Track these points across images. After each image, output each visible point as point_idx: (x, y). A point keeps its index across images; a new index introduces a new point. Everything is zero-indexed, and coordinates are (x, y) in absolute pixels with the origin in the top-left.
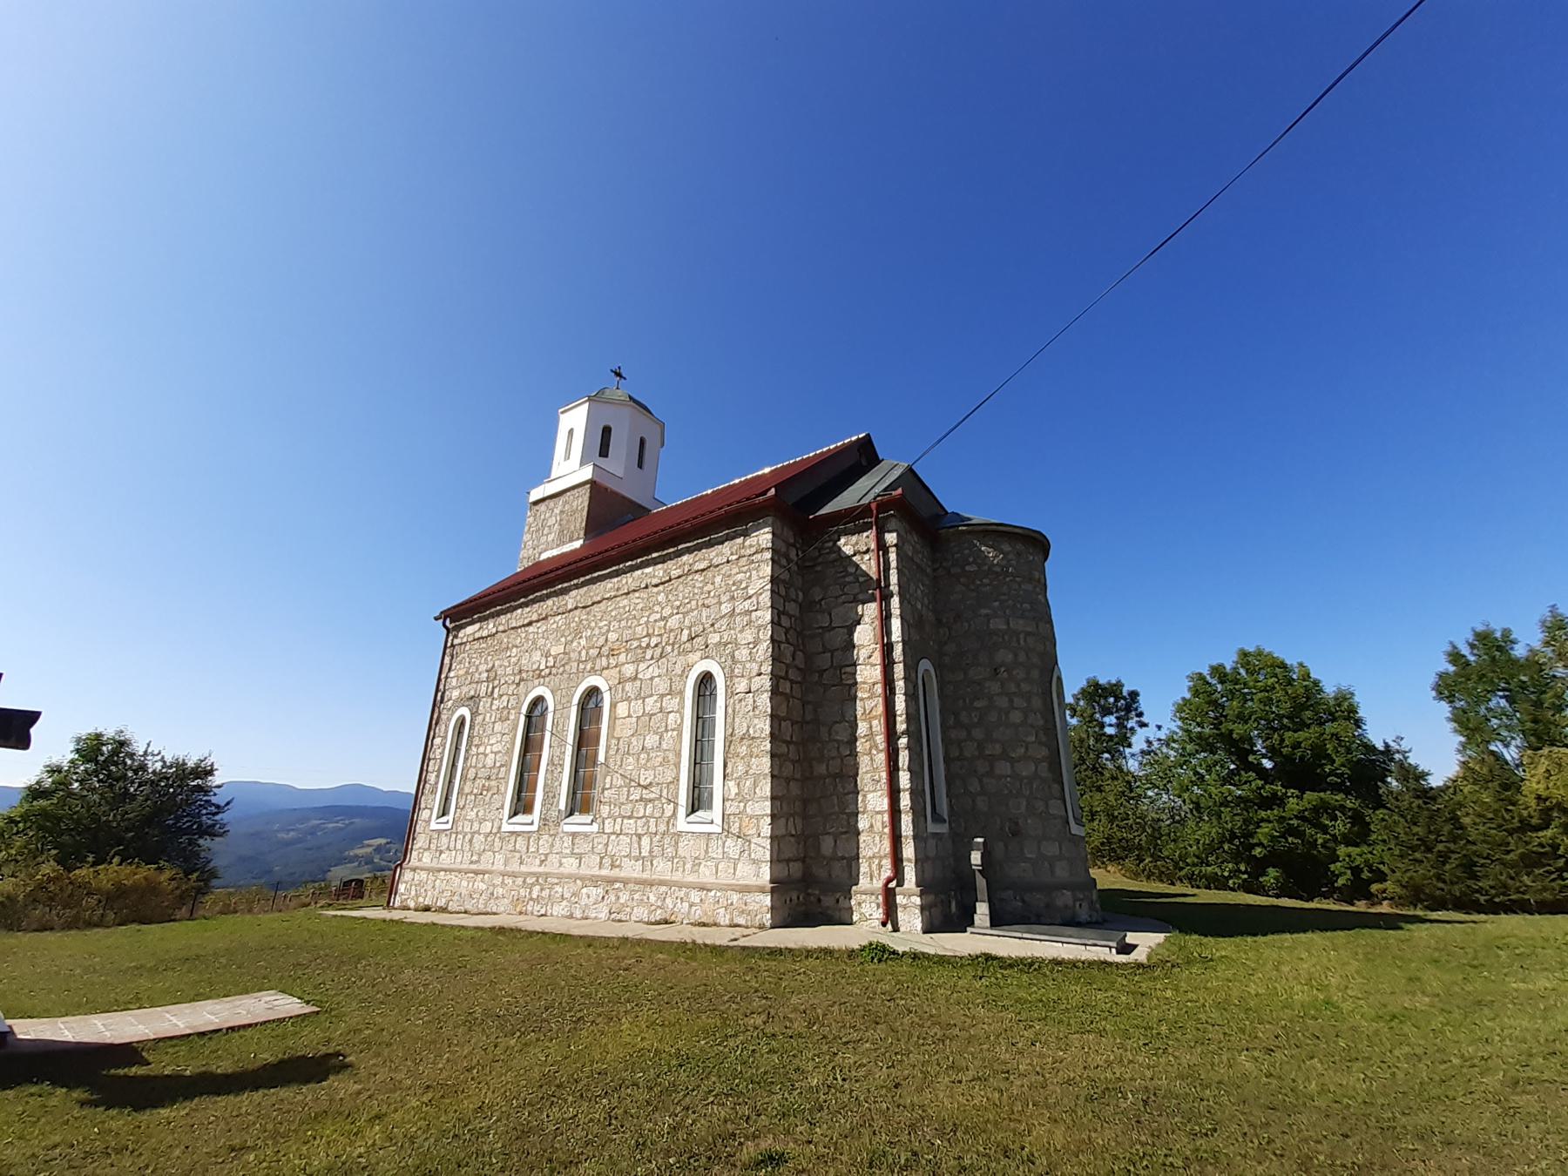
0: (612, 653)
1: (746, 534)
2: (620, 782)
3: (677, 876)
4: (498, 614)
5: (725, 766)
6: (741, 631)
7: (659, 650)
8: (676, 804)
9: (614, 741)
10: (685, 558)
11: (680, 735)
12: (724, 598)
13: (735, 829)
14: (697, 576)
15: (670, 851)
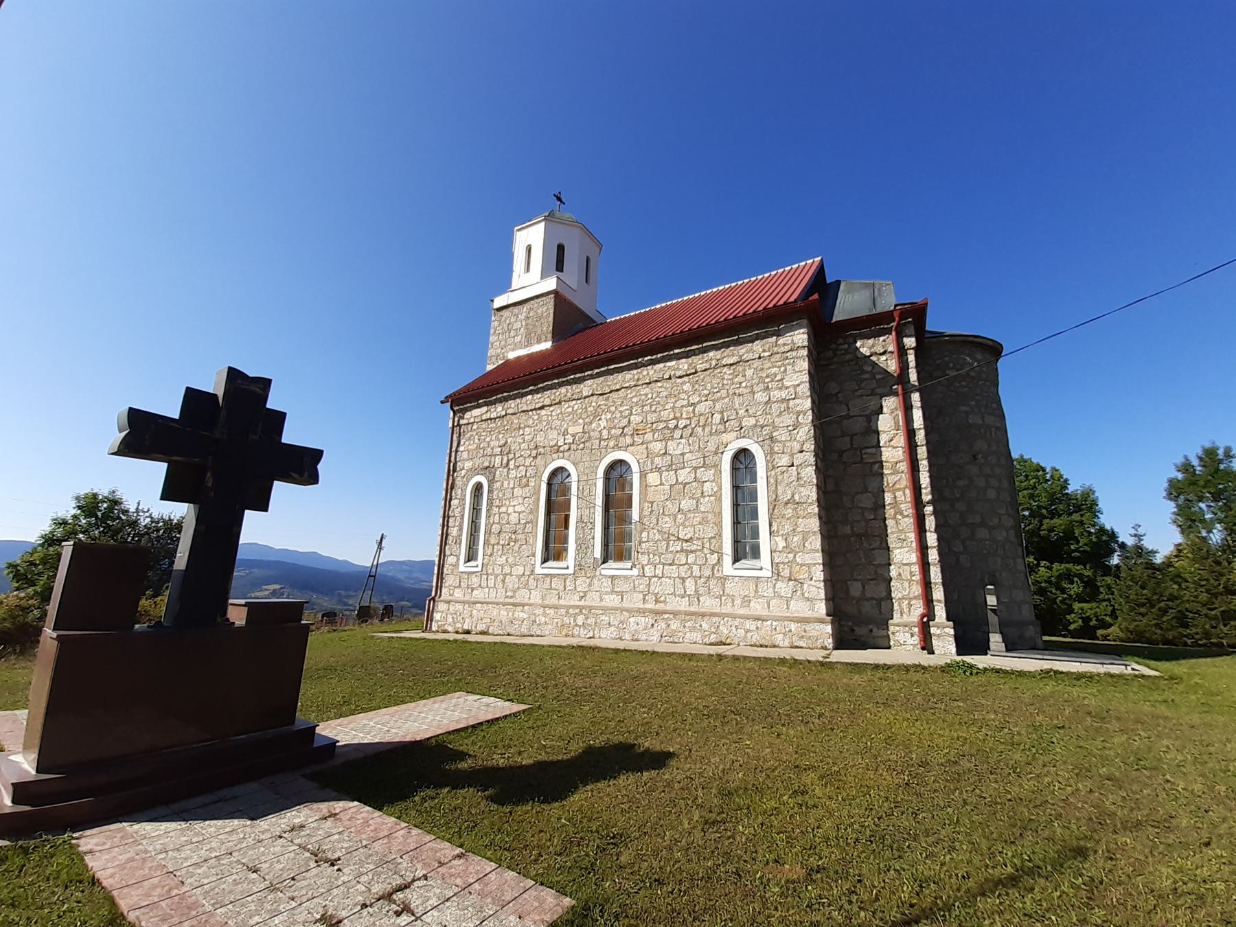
1: (778, 334)
2: (657, 537)
3: (728, 609)
4: (506, 399)
5: (771, 525)
6: (780, 415)
8: (720, 555)
10: (711, 354)
11: (719, 500)
13: (786, 573)
14: (725, 369)
15: (717, 590)
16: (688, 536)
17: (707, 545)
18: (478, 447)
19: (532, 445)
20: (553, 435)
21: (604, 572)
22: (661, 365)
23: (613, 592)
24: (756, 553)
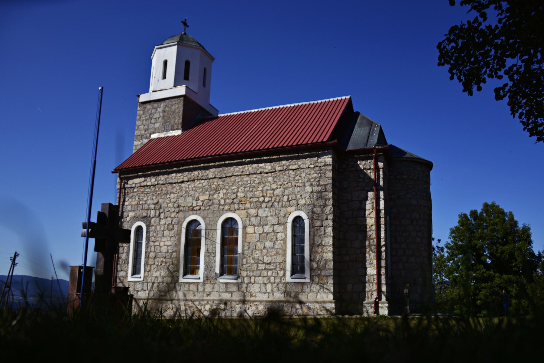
0: (241, 202)
1: (319, 156)
2: (252, 261)
4: (158, 174)
7: (270, 204)
9: (246, 244)
10: (284, 162)
12: (307, 184)
14: (291, 172)
16: (268, 262)
17: (278, 266)
18: (138, 204)
19: (176, 205)
20: (190, 199)
21: (221, 281)
22: (256, 165)
23: (226, 291)
24: (302, 271)
